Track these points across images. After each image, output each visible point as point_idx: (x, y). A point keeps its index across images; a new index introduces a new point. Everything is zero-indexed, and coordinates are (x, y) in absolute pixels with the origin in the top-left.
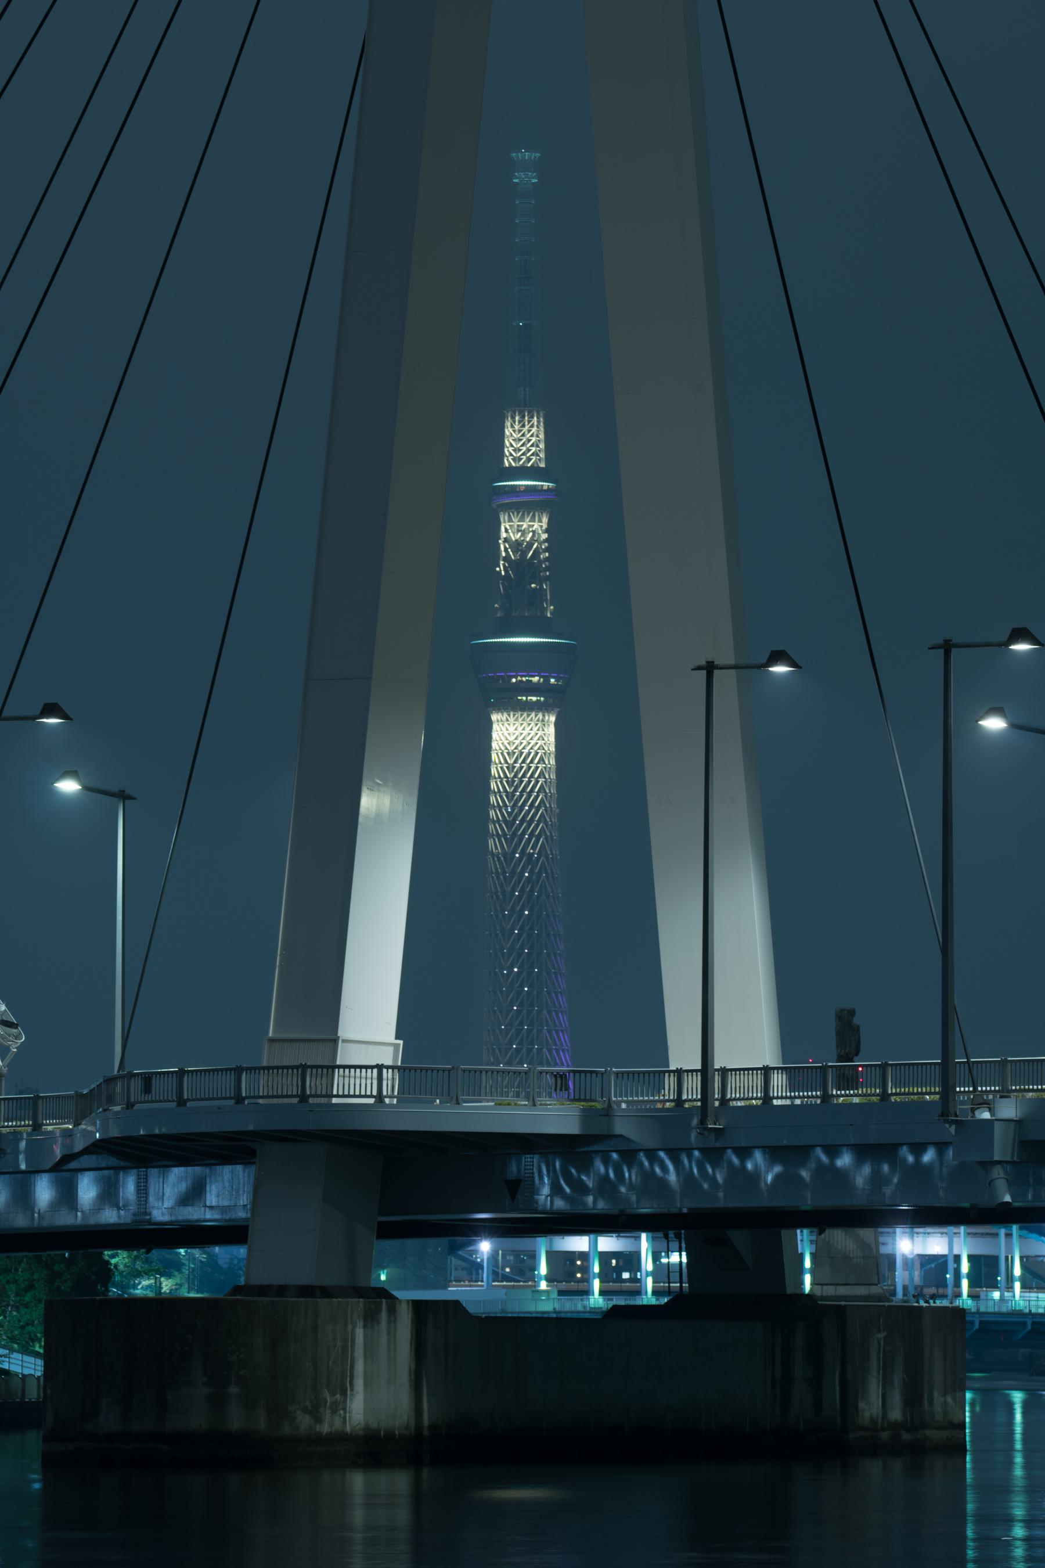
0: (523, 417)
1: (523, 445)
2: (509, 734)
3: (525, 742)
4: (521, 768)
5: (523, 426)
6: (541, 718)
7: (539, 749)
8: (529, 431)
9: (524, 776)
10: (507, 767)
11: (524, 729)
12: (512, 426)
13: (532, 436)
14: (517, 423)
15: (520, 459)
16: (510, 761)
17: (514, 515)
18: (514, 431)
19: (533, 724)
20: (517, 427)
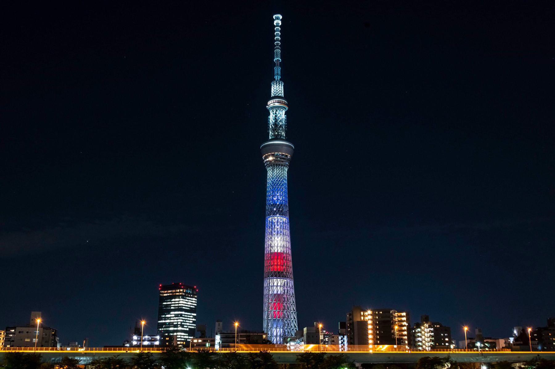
0: (277, 83)
7: (282, 177)
12: (274, 86)
15: (276, 95)
20: (275, 86)
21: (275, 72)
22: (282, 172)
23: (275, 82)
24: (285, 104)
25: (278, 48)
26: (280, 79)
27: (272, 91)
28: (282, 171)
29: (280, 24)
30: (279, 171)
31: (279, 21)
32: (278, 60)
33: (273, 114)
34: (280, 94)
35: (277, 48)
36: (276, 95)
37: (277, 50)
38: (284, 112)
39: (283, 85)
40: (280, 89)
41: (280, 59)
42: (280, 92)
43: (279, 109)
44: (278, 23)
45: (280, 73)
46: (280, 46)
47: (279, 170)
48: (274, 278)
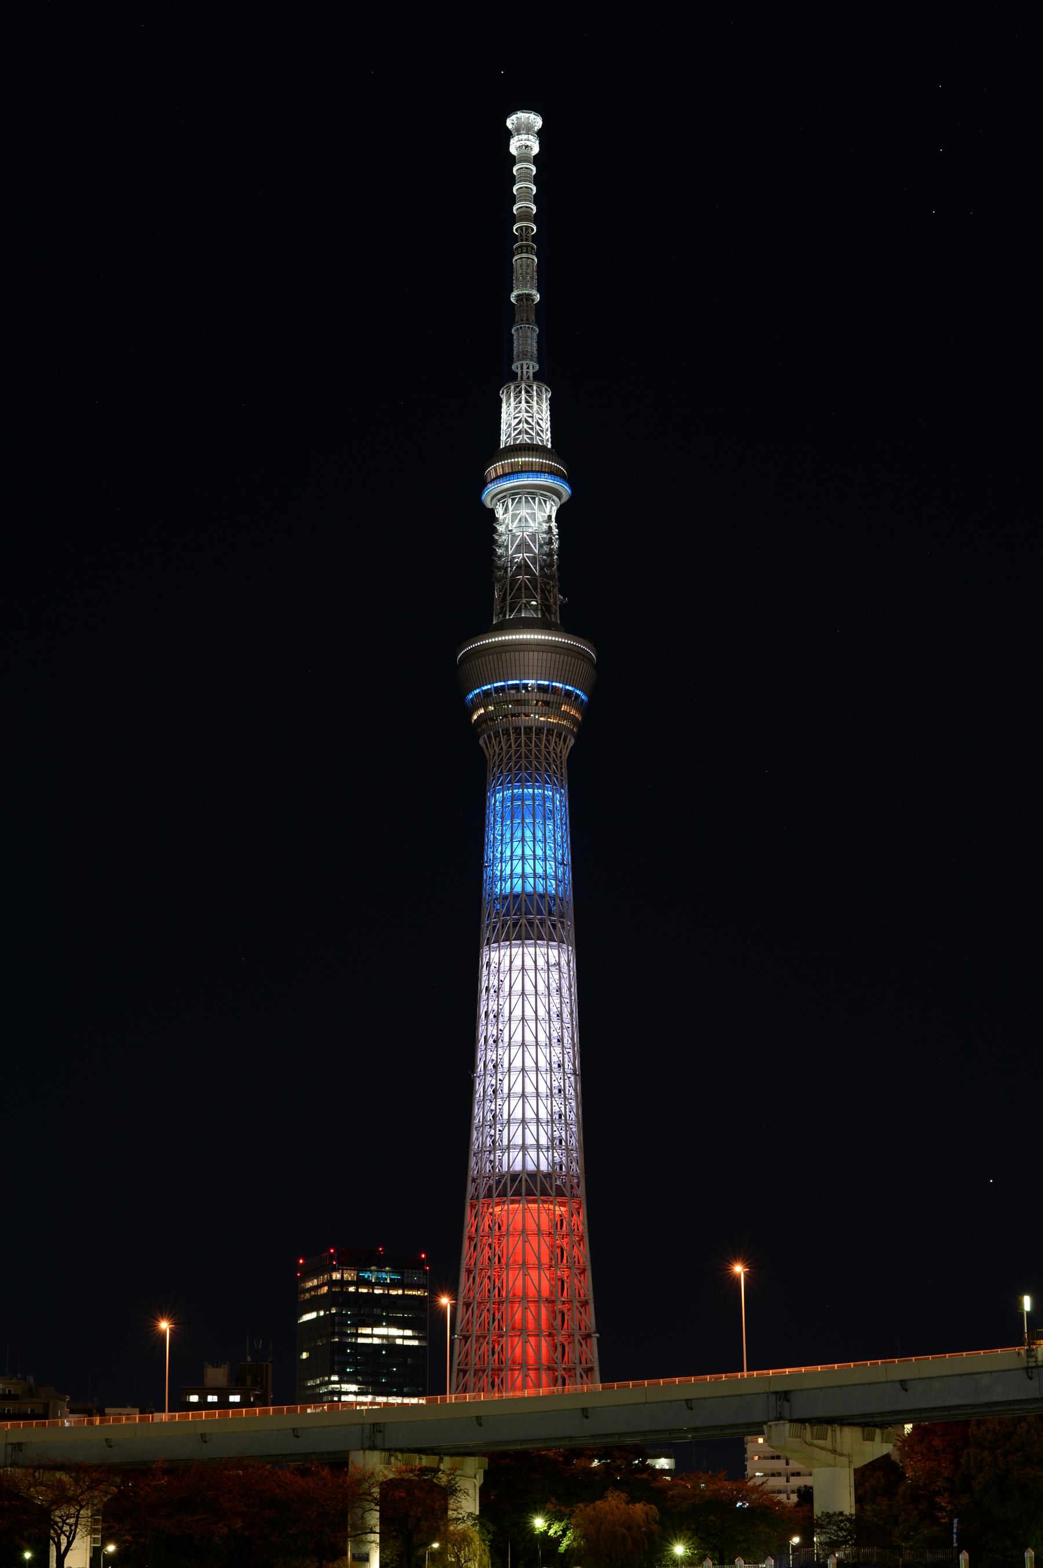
0: (520, 392)
5: (520, 403)
21: (515, 345)
23: (512, 387)
24: (552, 472)
25: (527, 249)
26: (537, 377)
27: (504, 427)
31: (531, 137)
34: (537, 441)
35: (527, 246)
36: (518, 442)
37: (524, 255)
38: (551, 509)
39: (547, 395)
41: (534, 292)
44: (527, 147)
45: (533, 346)
46: (534, 239)
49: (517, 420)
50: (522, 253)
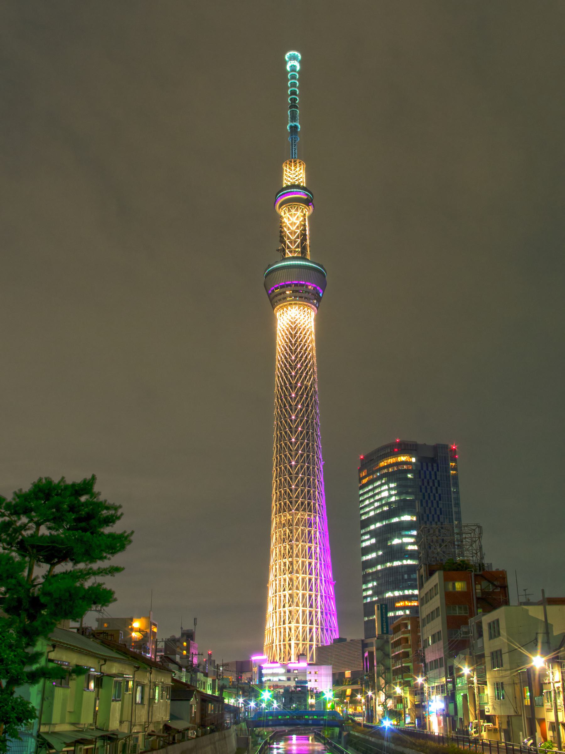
1: (296, 176)
2: (292, 318)
3: (302, 323)
4: (300, 337)
5: (296, 168)
6: (309, 313)
7: (309, 328)
8: (299, 171)
9: (301, 341)
10: (292, 337)
11: (301, 315)
12: (289, 168)
13: (301, 173)
14: (293, 166)
16: (293, 333)
17: (292, 209)
18: (291, 170)
19: (306, 314)
20: (293, 168)
22: (309, 320)
23: (293, 161)
28: (308, 318)
29: (298, 68)
30: (305, 316)
32: (296, 127)
33: (291, 215)
34: (302, 184)
36: (296, 184)
37: (293, 109)
40: (301, 175)
42: (301, 180)
43: (300, 208)
47: (304, 314)
48: (302, 513)
49: (295, 175)
50: (292, 108)
